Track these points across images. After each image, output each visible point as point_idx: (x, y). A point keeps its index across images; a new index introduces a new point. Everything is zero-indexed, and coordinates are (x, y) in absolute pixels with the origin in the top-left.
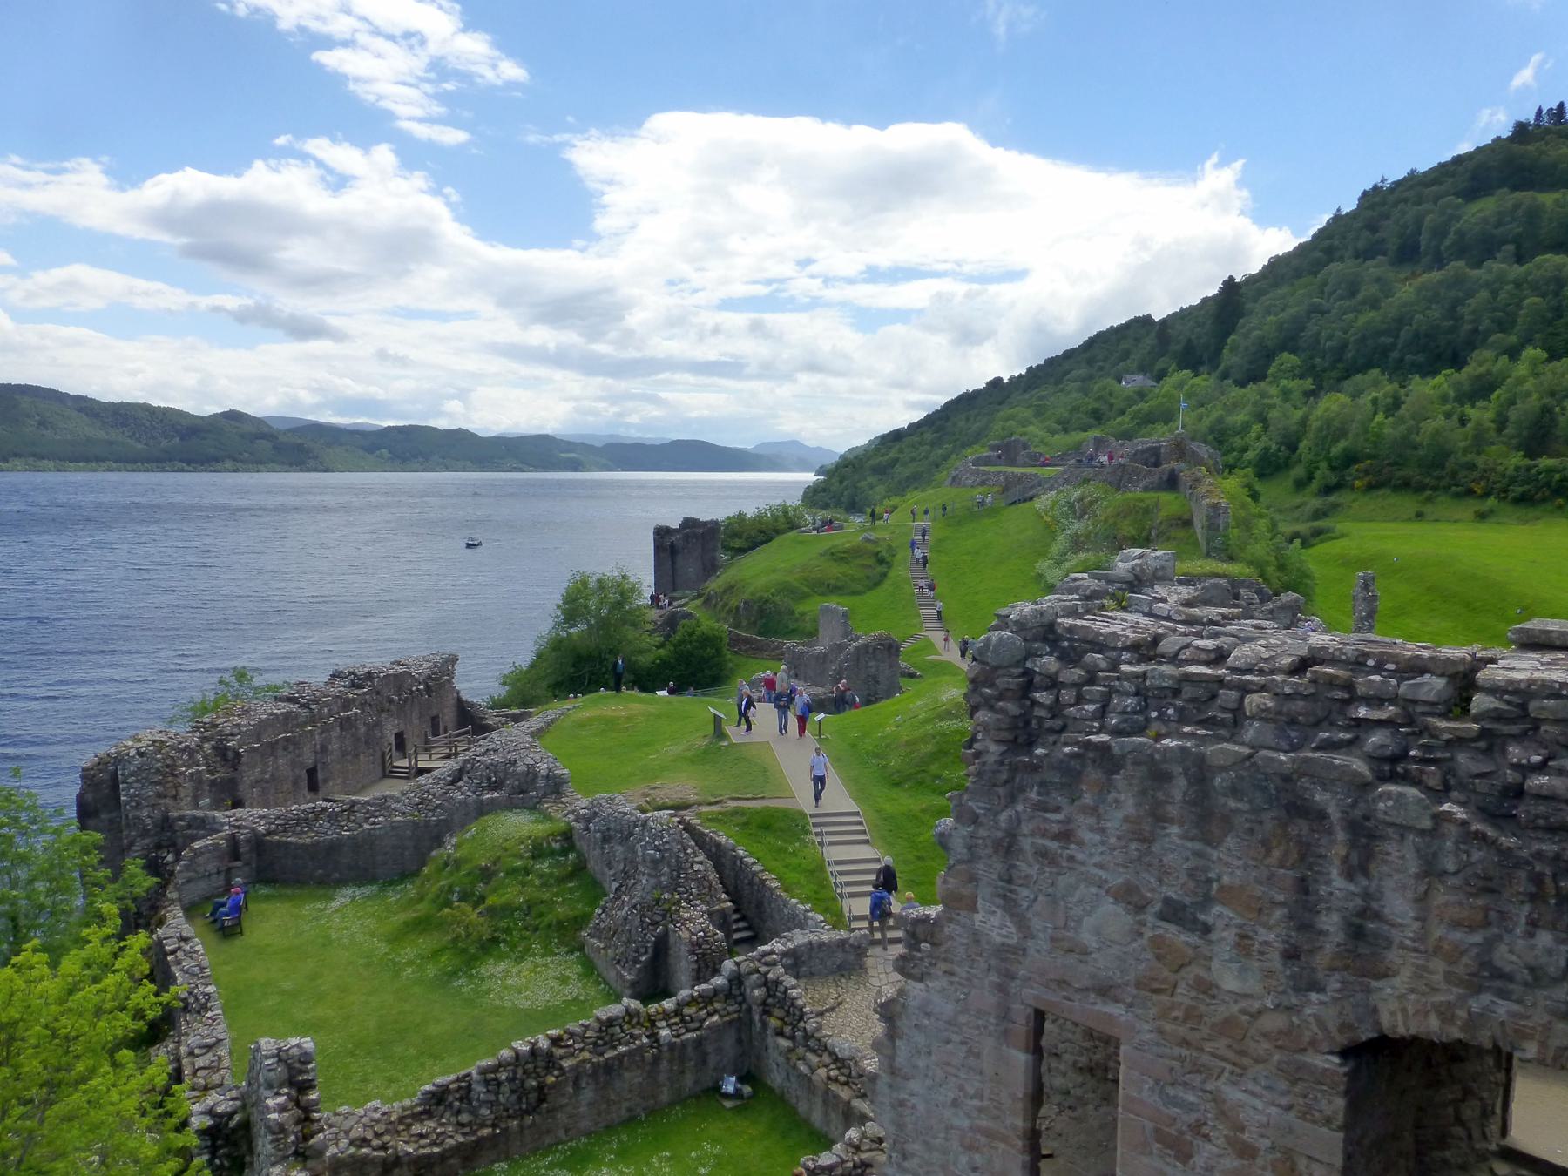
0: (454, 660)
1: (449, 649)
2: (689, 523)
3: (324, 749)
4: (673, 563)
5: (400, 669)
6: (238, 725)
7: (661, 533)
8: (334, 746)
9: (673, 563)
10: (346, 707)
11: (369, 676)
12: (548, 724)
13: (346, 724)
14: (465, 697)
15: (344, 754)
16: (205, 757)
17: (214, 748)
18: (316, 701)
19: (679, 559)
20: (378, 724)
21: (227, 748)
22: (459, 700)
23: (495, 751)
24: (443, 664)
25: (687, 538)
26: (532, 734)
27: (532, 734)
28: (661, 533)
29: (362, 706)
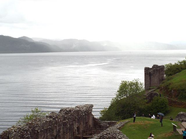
0: (92, 106)
1: (92, 103)
2: (155, 66)
3: (59, 131)
4: (150, 78)
5: (78, 109)
6: (38, 124)
7: (147, 70)
8: (62, 130)
9: (150, 78)
10: (64, 120)
11: (70, 111)
12: (122, 126)
13: (65, 124)
14: (95, 117)
15: (64, 132)
16: (30, 133)
17: (32, 130)
18: (57, 118)
19: (152, 77)
20: (73, 124)
21: (35, 130)
22: (94, 118)
23: (109, 134)
24: (89, 108)
25: (154, 71)
26: (119, 129)
27: (119, 129)
28: (147, 70)
29: (68, 119)
